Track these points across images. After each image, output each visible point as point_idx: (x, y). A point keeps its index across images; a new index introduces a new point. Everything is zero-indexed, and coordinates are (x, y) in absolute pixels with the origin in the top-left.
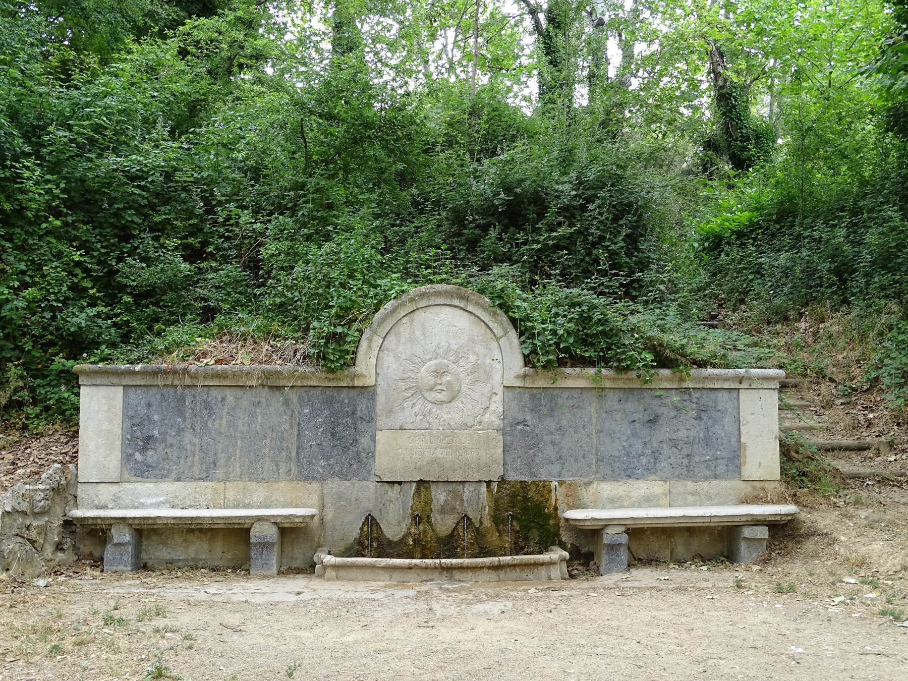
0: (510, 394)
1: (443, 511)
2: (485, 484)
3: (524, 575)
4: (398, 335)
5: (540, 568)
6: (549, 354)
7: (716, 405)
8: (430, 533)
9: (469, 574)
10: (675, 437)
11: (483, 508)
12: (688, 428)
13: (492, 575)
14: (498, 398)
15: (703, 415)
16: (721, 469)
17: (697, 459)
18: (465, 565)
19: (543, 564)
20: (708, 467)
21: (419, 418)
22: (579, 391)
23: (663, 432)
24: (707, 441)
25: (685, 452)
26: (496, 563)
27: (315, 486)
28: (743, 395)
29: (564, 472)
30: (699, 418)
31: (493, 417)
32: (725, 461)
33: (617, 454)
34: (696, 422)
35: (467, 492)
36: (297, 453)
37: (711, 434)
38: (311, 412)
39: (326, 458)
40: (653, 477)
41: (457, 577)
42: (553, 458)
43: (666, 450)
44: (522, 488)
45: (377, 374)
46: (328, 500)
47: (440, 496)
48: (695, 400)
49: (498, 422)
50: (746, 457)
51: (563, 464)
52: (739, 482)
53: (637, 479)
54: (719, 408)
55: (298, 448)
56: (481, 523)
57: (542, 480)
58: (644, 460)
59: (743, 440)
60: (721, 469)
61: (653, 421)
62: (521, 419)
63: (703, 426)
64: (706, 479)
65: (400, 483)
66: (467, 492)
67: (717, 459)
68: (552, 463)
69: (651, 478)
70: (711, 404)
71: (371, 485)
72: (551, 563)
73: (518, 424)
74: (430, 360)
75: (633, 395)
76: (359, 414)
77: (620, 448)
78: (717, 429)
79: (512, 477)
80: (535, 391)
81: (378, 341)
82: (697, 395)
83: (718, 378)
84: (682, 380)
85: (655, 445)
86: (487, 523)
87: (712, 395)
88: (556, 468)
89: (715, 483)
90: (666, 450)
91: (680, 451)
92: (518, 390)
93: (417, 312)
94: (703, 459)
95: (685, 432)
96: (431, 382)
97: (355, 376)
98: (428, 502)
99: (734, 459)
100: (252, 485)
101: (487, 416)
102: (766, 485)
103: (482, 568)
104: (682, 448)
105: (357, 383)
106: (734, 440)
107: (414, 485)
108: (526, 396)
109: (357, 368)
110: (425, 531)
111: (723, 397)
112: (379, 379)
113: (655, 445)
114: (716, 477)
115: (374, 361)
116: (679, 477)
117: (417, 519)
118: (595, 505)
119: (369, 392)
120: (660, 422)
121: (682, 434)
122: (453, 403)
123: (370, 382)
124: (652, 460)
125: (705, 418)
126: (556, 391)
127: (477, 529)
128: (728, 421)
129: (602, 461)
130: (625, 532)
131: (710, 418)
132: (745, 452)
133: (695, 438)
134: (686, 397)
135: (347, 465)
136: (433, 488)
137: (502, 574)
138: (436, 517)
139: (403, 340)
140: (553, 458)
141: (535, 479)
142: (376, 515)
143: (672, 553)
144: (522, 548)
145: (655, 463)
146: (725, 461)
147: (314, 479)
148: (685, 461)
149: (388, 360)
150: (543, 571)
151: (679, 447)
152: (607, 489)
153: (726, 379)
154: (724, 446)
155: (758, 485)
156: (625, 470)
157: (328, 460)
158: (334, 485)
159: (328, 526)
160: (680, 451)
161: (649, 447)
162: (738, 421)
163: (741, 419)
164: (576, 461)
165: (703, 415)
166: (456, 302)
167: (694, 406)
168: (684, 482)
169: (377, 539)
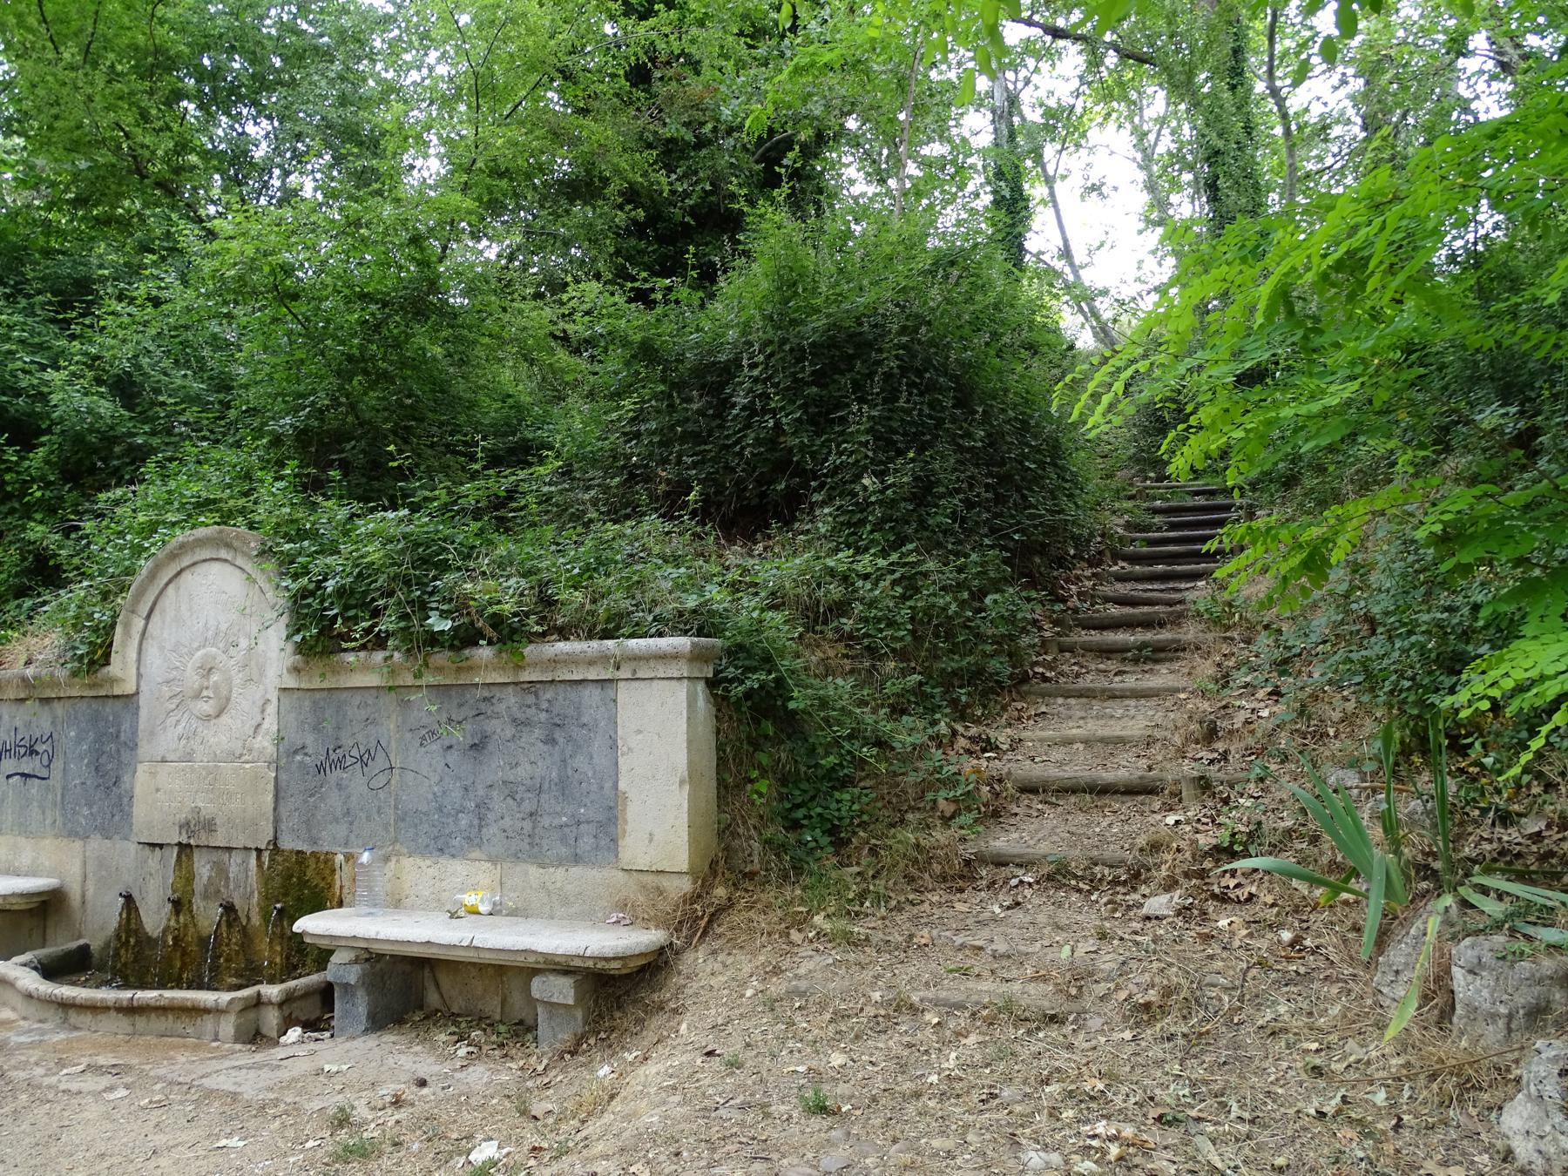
0: (286, 701)
1: (206, 896)
2: (254, 854)
3: (179, 1026)
4: (163, 611)
5: (205, 1017)
6: (322, 627)
7: (579, 715)
8: (192, 930)
9: (87, 1019)
10: (512, 778)
11: (252, 892)
12: (530, 760)
13: (123, 1023)
14: (271, 709)
15: (559, 735)
16: (586, 843)
17: (546, 821)
18: (78, 1001)
19: (206, 1011)
20: (564, 840)
21: (183, 742)
22: (374, 692)
23: (495, 768)
24: (564, 786)
25: (528, 806)
26: (125, 1003)
27: (78, 844)
28: (624, 693)
29: (352, 836)
30: (550, 741)
31: (264, 744)
32: (591, 828)
33: (423, 807)
34: (545, 748)
35: (234, 863)
36: (63, 796)
37: (570, 772)
38: (77, 736)
39: (90, 805)
40: (476, 854)
41: (72, 1020)
42: (339, 813)
43: (498, 804)
44: (297, 862)
45: (139, 676)
46: (89, 869)
47: (203, 868)
48: (545, 705)
49: (270, 750)
50: (626, 822)
51: (351, 823)
52: (615, 872)
53: (453, 856)
54: (585, 720)
55: (64, 788)
56: (249, 919)
57: (326, 849)
58: (464, 821)
59: (622, 786)
60: (586, 843)
61: (478, 747)
62: (299, 744)
63: (557, 757)
64: (560, 862)
65: (161, 846)
66: (234, 863)
67: (579, 823)
68: (336, 820)
69: (473, 855)
70: (571, 712)
71: (130, 850)
72: (217, 1011)
73: (296, 752)
74: (198, 649)
75: (450, 697)
76: (123, 738)
77: (430, 796)
78: (580, 762)
79: (287, 843)
80: (318, 695)
81: (139, 623)
82: (548, 696)
83: (572, 661)
84: (519, 667)
85: (481, 792)
86: (256, 920)
87: (572, 694)
88: (341, 830)
89: (576, 871)
90: (498, 804)
91: (519, 805)
92: (296, 695)
93: (184, 575)
94: (556, 822)
95: (528, 767)
96: (196, 686)
97: (113, 681)
98: (190, 879)
99: (608, 825)
100: (22, 841)
101: (259, 738)
102: (665, 882)
103: (107, 1008)
104: (522, 799)
105: (117, 692)
106: (608, 785)
107: (176, 850)
108: (307, 703)
109: (110, 668)
110: (186, 926)
111: (591, 696)
112: (142, 684)
113: (481, 792)
114: (577, 859)
115: (134, 656)
116: (517, 857)
117: (177, 905)
118: (396, 903)
119: (129, 700)
120: (490, 747)
121: (523, 771)
122: (224, 719)
123: (130, 688)
124: (476, 822)
125: (561, 740)
126: (345, 695)
127: (244, 928)
128: (598, 744)
129: (403, 820)
130: (356, 961)
131: (569, 739)
132: (624, 810)
133: (543, 778)
134: (531, 699)
135: (108, 816)
136: (196, 855)
137: (141, 1022)
138: (198, 903)
139: (168, 619)
140: (339, 813)
141: (315, 849)
142: (136, 895)
143: (504, 1002)
144: (295, 968)
145: (480, 827)
146: (591, 828)
147: (77, 834)
148: (527, 825)
149: (152, 653)
150: (208, 1023)
151: (518, 797)
152: (416, 872)
153: (591, 663)
154: (592, 796)
155: (648, 879)
156: (436, 838)
157: (90, 808)
158: (96, 844)
159: (89, 906)
160: (519, 805)
161: (471, 795)
162: (614, 746)
163: (620, 743)
164: (368, 819)
165: (559, 735)
166: (223, 554)
167: (543, 716)
168: (524, 866)
169: (136, 931)
